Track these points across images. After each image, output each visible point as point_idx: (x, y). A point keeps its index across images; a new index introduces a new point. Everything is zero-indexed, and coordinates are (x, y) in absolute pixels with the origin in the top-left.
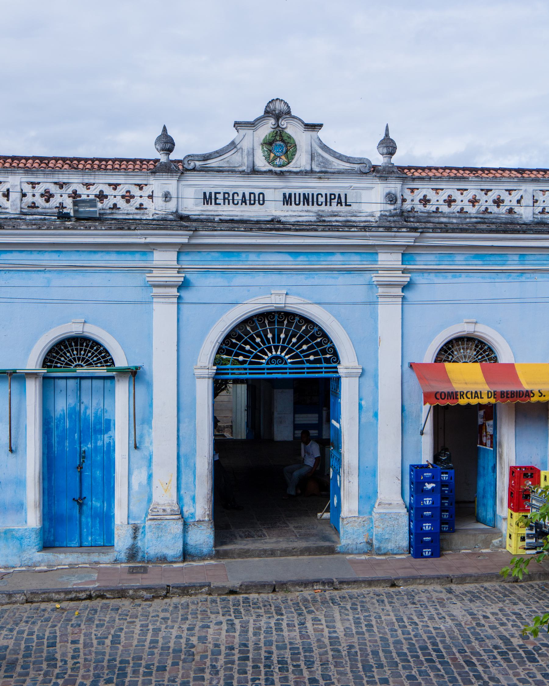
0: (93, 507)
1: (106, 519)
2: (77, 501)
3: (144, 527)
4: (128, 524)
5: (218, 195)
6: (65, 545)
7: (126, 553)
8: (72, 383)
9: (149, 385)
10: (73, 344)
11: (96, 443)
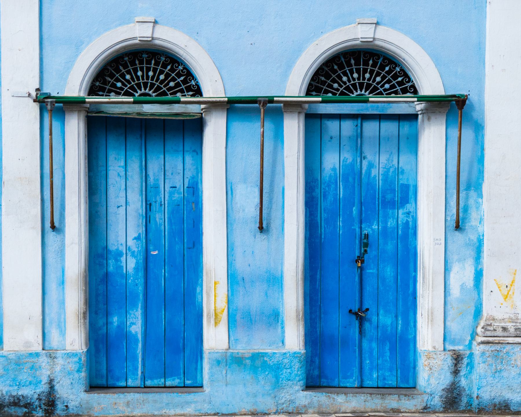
0: (381, 325)
1: (402, 344)
2: (356, 314)
3: (471, 355)
4: (444, 350)
6: (336, 383)
7: (441, 397)
8: (348, 126)
9: (479, 128)
10: (353, 62)
11: (386, 223)
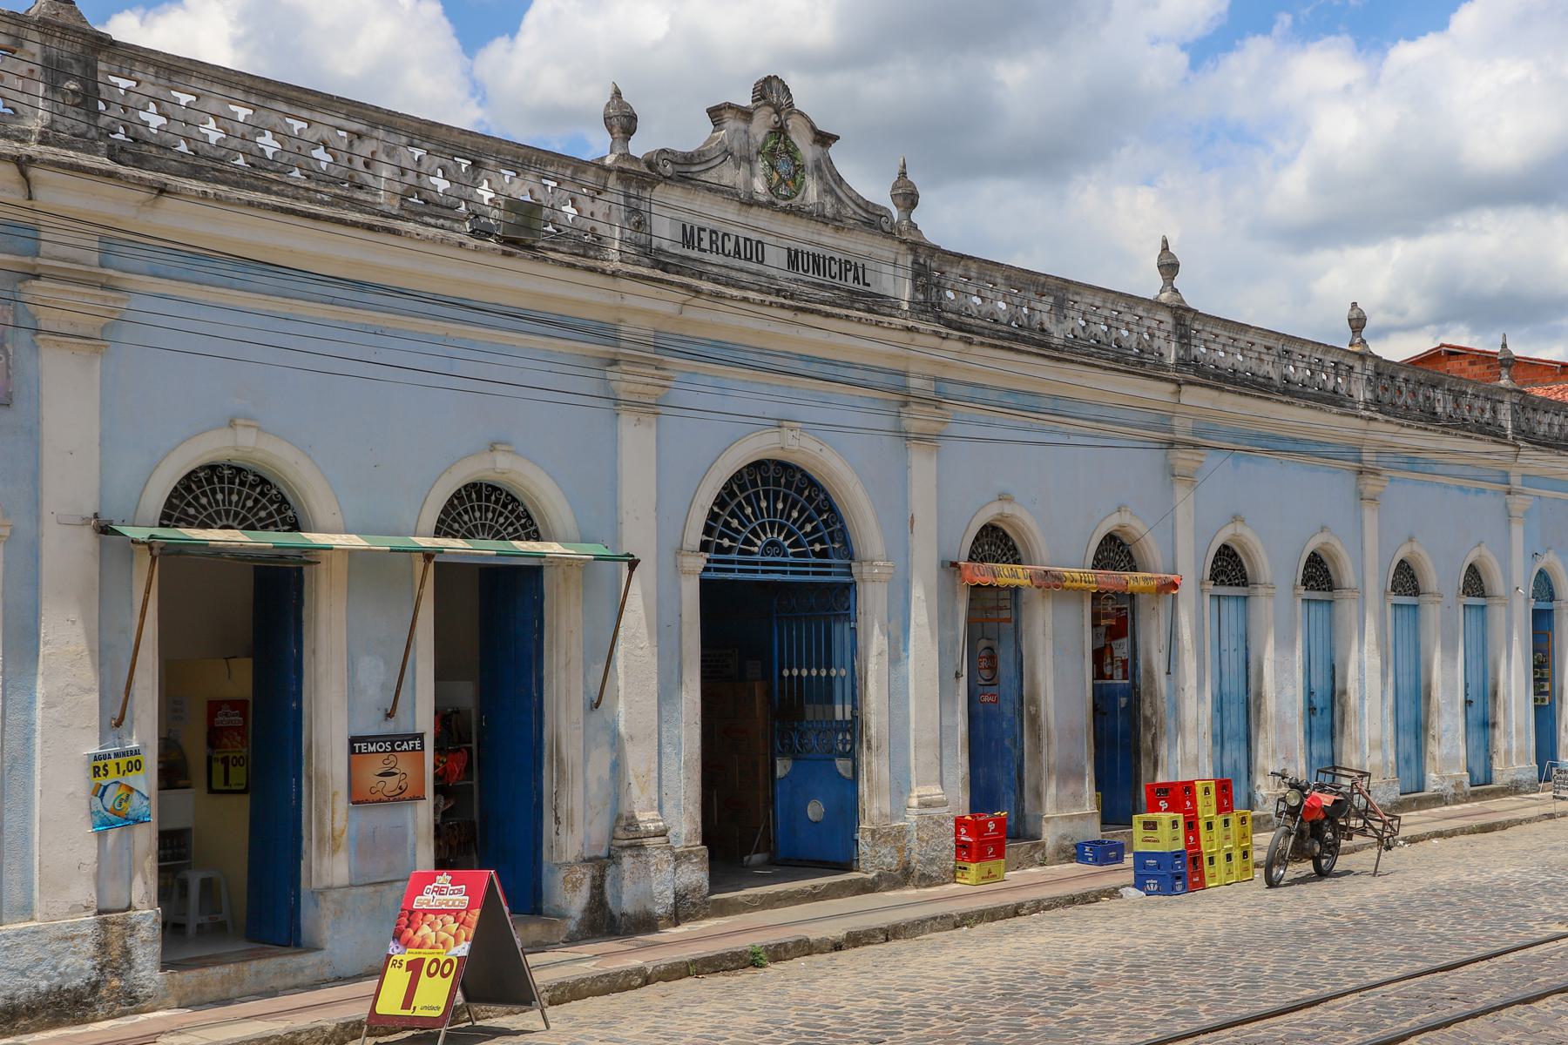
5: (703, 234)
